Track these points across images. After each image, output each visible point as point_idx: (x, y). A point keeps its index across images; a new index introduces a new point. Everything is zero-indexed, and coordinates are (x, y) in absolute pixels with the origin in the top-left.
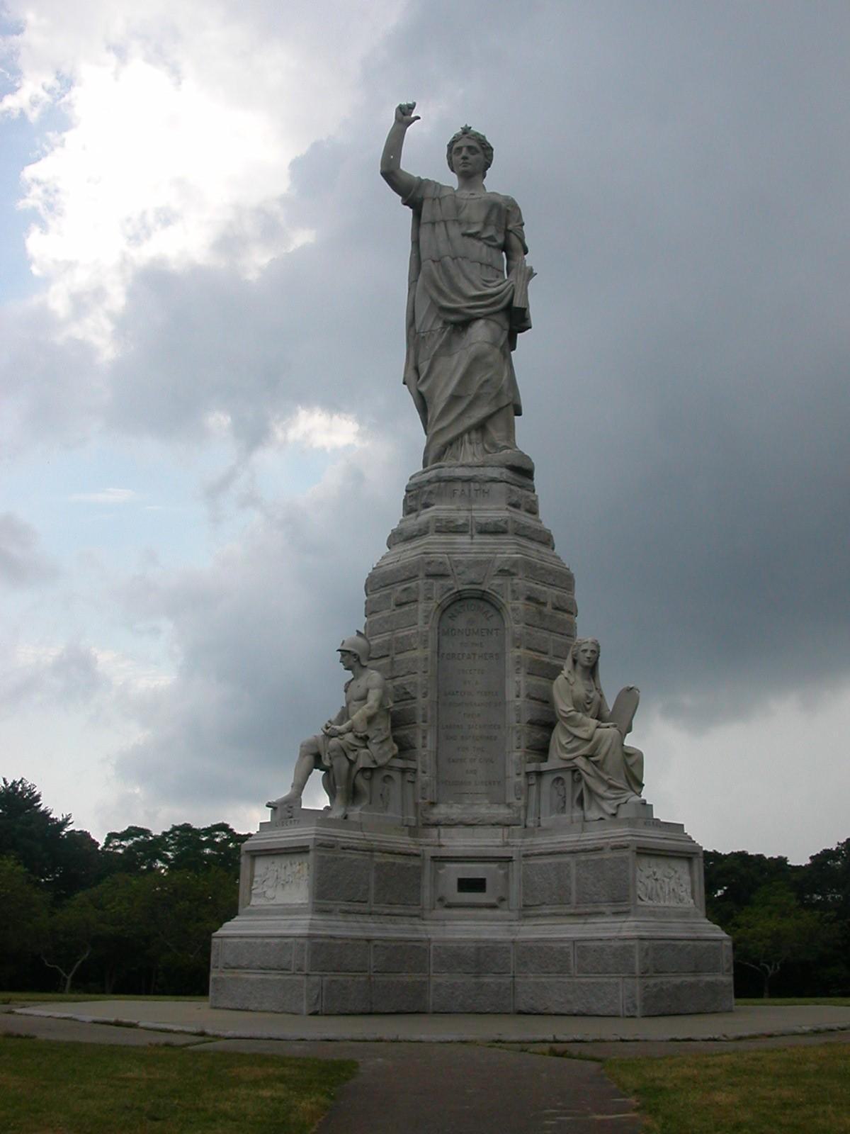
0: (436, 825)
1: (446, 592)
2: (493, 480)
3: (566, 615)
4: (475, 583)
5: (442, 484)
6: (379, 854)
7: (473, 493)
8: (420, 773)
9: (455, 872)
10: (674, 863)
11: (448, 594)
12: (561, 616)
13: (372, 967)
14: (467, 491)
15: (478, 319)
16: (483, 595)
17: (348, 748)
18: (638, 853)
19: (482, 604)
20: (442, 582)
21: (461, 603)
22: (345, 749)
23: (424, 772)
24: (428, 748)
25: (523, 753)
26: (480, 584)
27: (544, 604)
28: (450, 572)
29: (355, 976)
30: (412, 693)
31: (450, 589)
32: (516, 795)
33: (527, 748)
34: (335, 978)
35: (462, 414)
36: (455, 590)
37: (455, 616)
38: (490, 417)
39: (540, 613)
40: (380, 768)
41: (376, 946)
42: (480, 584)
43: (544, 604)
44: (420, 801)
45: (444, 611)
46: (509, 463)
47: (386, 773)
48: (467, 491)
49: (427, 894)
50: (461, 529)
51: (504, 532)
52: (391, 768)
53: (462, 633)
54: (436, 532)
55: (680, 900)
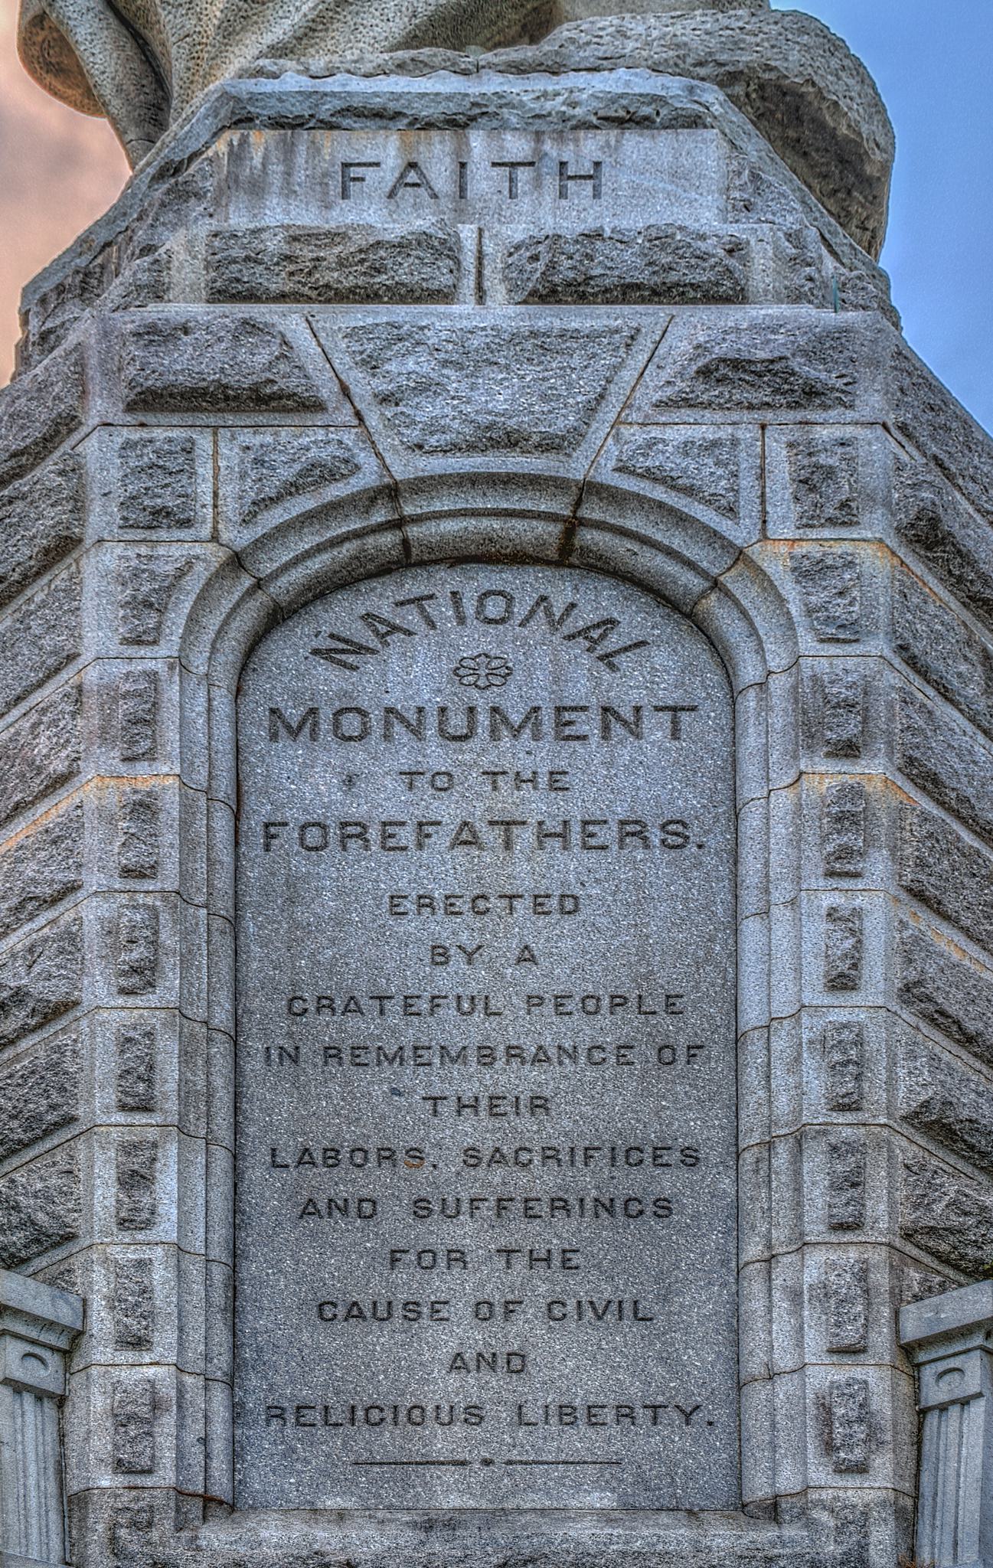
1: (293, 489)
4: (512, 441)
5: (261, 141)
7: (484, 181)
8: (101, 1351)
14: (440, 174)
16: (572, 525)
19: (562, 590)
21: (414, 585)
23: (138, 1343)
24: (167, 1228)
26: (550, 445)
28: (328, 391)
30: (39, 989)
32: (829, 1447)
33: (908, 1236)
36: (368, 477)
37: (360, 649)
42: (550, 445)
44: (106, 1480)
45: (277, 617)
48: (440, 174)
50: (405, 272)
53: (417, 731)
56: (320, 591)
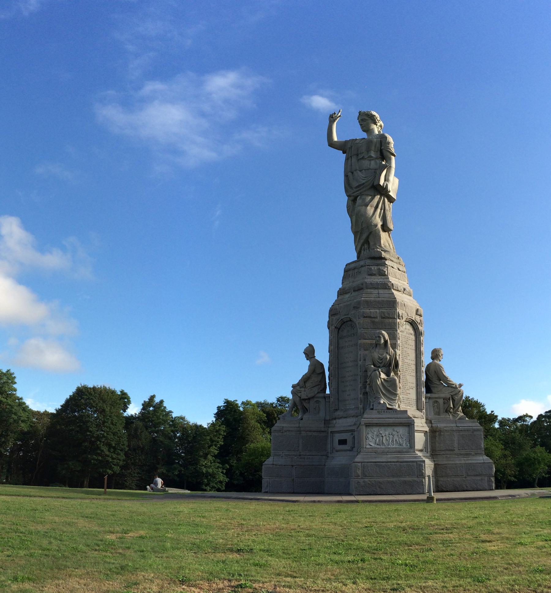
0: (335, 419)
2: (362, 266)
3: (391, 320)
6: (304, 432)
9: (338, 437)
10: (396, 429)
11: (338, 322)
12: (387, 321)
13: (294, 475)
14: (353, 274)
15: (358, 196)
17: (298, 392)
18: (366, 426)
20: (336, 317)
22: (296, 393)
25: (362, 385)
26: (347, 315)
27: (376, 318)
29: (286, 479)
31: (338, 320)
34: (276, 480)
35: (359, 239)
36: (340, 320)
38: (368, 237)
39: (373, 322)
40: (313, 397)
41: (295, 468)
43: (376, 318)
45: (339, 329)
46: (369, 257)
47: (316, 399)
48: (353, 274)
49: (329, 446)
51: (362, 289)
52: (317, 397)
54: (340, 295)
55: (400, 444)
56: (341, 326)
